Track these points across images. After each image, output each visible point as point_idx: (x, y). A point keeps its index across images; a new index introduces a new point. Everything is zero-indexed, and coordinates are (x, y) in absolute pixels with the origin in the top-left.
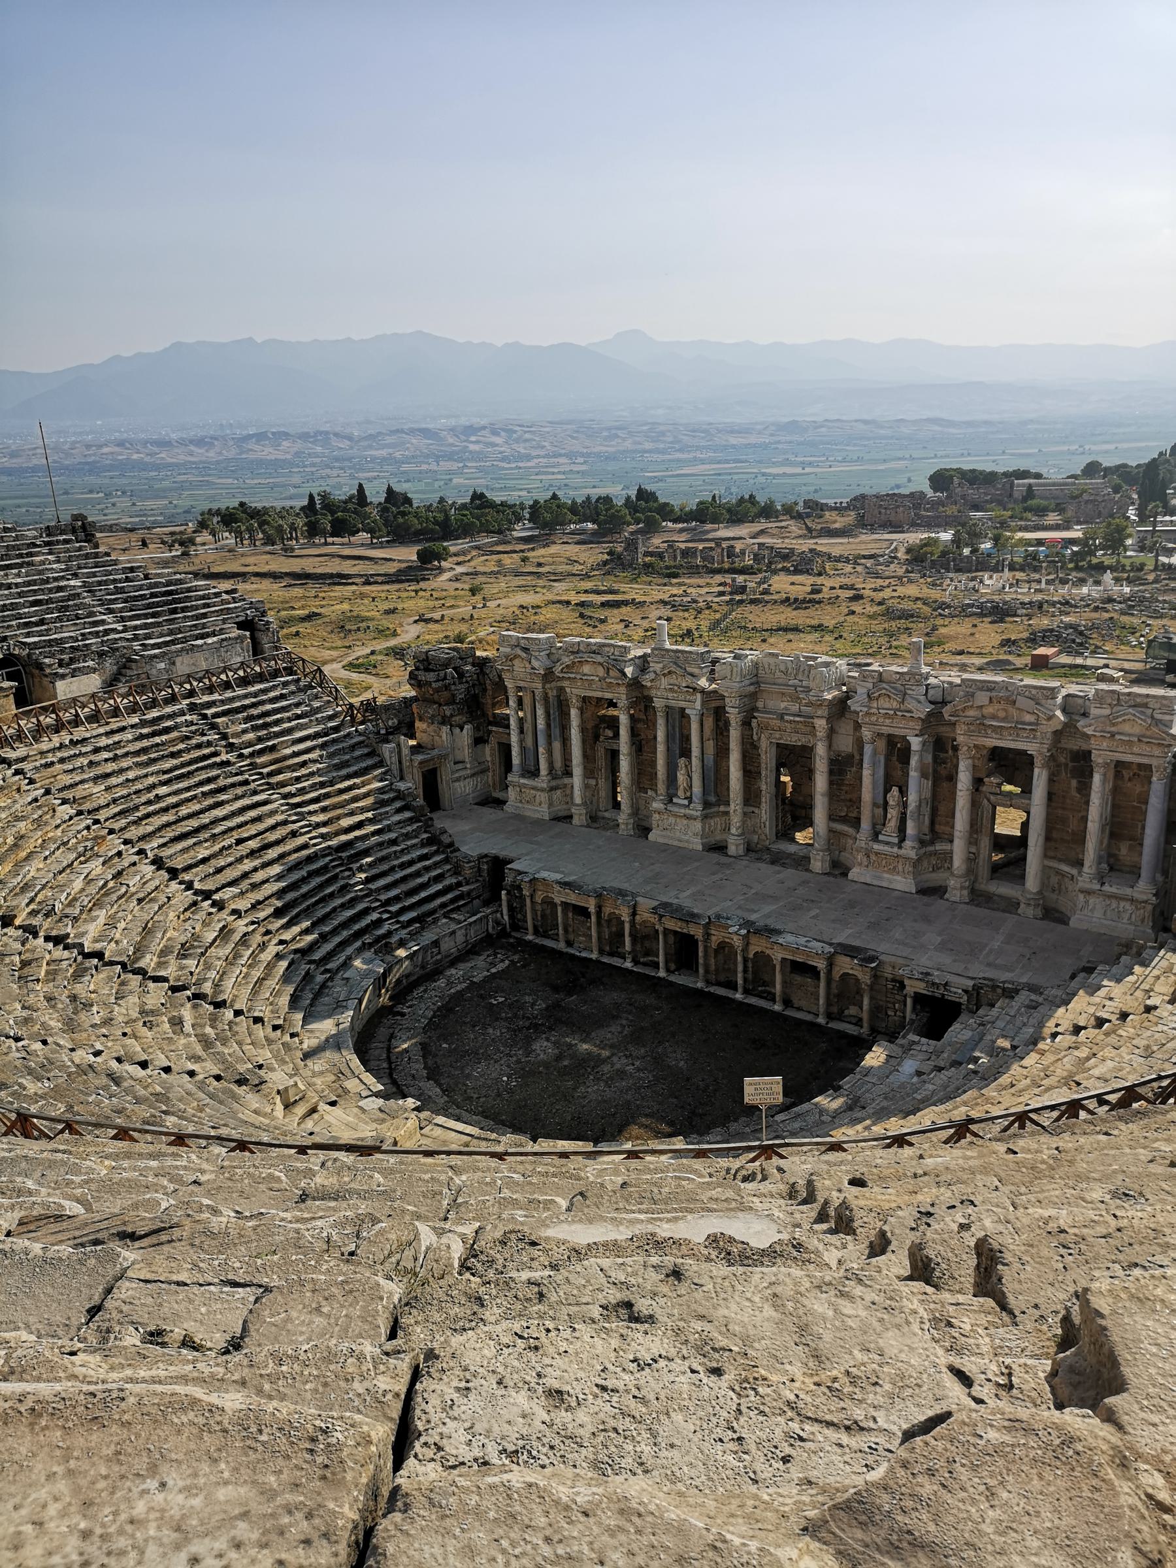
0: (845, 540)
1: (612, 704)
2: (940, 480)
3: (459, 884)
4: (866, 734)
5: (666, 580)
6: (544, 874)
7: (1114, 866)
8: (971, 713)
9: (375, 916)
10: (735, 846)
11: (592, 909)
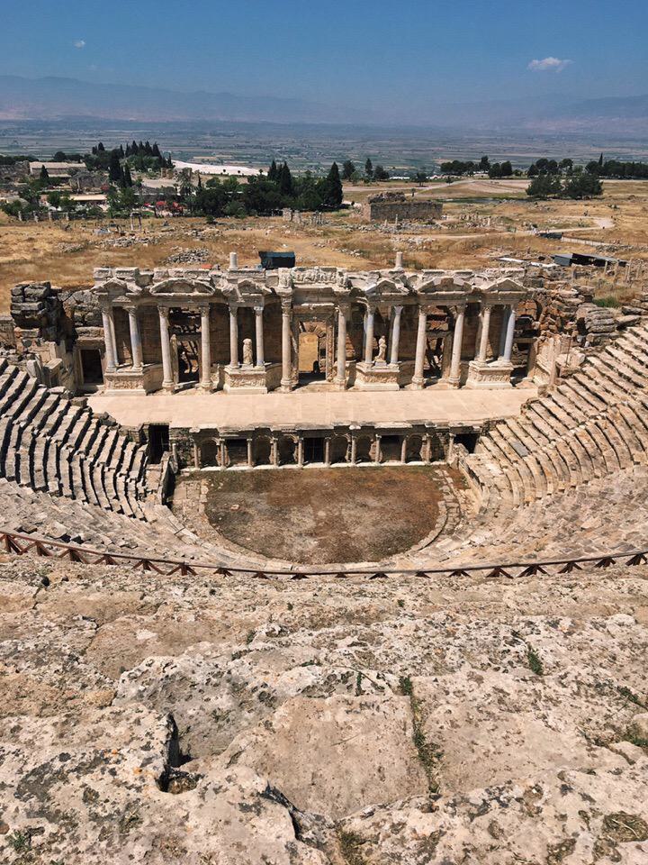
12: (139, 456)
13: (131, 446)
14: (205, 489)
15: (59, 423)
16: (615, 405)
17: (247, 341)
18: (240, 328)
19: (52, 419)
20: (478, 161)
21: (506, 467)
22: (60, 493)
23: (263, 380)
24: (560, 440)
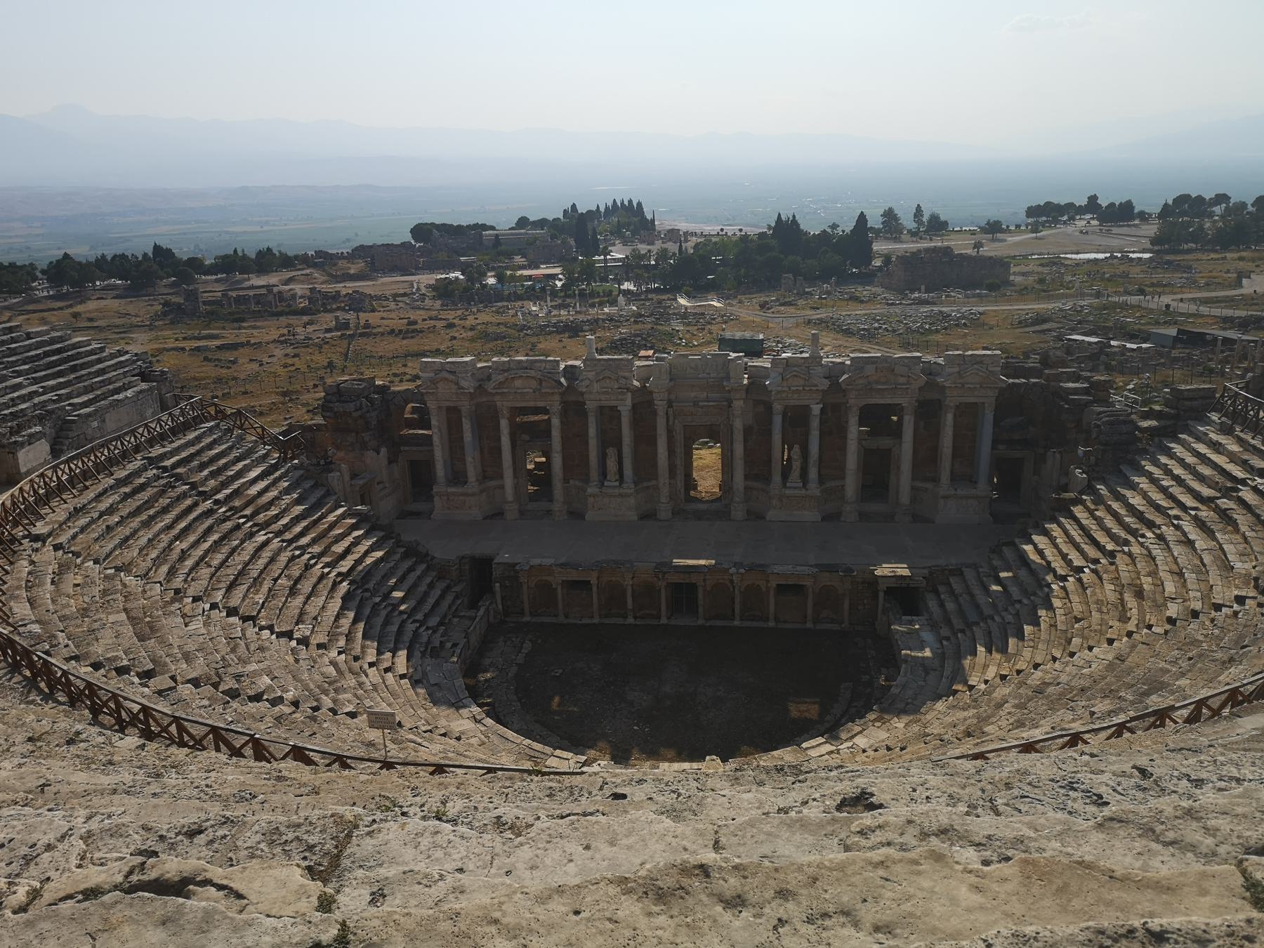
0: (370, 283)
1: (544, 411)
2: (420, 231)
3: (448, 588)
4: (778, 407)
5: (236, 325)
6: (536, 561)
7: (963, 477)
8: (861, 381)
9: (411, 627)
10: (664, 511)
11: (594, 581)
12: (449, 598)
13: (441, 585)
14: (528, 646)
15: (347, 551)
16: (1111, 555)
17: (611, 452)
18: (602, 433)
19: (339, 548)
20: (1082, 201)
21: (948, 639)
22: (304, 641)
23: (632, 501)
24: (1025, 601)
